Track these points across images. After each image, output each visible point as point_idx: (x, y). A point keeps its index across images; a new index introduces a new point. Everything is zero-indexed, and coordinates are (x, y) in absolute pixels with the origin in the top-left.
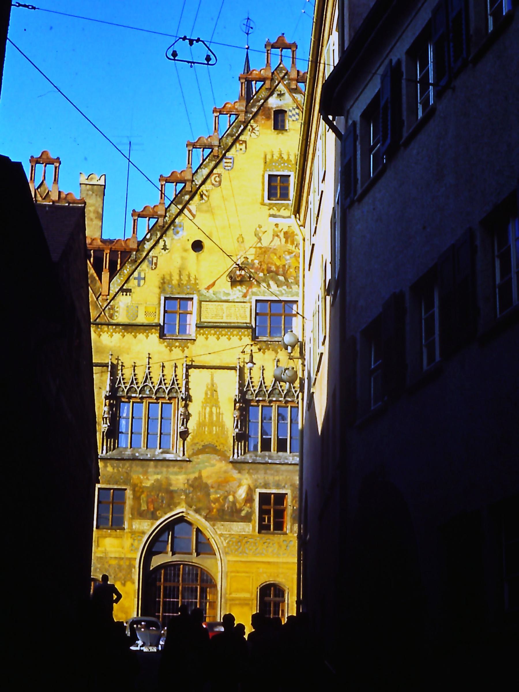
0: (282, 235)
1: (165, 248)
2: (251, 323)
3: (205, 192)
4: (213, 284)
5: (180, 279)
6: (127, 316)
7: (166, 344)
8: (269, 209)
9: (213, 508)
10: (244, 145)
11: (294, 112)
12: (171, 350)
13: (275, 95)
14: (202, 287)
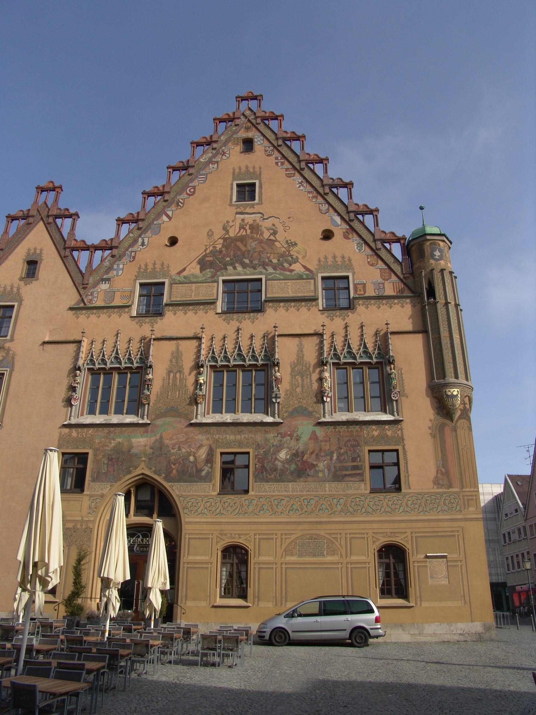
0: (247, 227)
1: (143, 244)
2: (217, 299)
3: (180, 200)
4: (184, 270)
5: (154, 268)
6: (105, 300)
7: (136, 320)
9: (173, 469)
10: (216, 165)
11: (259, 139)
14: (173, 272)
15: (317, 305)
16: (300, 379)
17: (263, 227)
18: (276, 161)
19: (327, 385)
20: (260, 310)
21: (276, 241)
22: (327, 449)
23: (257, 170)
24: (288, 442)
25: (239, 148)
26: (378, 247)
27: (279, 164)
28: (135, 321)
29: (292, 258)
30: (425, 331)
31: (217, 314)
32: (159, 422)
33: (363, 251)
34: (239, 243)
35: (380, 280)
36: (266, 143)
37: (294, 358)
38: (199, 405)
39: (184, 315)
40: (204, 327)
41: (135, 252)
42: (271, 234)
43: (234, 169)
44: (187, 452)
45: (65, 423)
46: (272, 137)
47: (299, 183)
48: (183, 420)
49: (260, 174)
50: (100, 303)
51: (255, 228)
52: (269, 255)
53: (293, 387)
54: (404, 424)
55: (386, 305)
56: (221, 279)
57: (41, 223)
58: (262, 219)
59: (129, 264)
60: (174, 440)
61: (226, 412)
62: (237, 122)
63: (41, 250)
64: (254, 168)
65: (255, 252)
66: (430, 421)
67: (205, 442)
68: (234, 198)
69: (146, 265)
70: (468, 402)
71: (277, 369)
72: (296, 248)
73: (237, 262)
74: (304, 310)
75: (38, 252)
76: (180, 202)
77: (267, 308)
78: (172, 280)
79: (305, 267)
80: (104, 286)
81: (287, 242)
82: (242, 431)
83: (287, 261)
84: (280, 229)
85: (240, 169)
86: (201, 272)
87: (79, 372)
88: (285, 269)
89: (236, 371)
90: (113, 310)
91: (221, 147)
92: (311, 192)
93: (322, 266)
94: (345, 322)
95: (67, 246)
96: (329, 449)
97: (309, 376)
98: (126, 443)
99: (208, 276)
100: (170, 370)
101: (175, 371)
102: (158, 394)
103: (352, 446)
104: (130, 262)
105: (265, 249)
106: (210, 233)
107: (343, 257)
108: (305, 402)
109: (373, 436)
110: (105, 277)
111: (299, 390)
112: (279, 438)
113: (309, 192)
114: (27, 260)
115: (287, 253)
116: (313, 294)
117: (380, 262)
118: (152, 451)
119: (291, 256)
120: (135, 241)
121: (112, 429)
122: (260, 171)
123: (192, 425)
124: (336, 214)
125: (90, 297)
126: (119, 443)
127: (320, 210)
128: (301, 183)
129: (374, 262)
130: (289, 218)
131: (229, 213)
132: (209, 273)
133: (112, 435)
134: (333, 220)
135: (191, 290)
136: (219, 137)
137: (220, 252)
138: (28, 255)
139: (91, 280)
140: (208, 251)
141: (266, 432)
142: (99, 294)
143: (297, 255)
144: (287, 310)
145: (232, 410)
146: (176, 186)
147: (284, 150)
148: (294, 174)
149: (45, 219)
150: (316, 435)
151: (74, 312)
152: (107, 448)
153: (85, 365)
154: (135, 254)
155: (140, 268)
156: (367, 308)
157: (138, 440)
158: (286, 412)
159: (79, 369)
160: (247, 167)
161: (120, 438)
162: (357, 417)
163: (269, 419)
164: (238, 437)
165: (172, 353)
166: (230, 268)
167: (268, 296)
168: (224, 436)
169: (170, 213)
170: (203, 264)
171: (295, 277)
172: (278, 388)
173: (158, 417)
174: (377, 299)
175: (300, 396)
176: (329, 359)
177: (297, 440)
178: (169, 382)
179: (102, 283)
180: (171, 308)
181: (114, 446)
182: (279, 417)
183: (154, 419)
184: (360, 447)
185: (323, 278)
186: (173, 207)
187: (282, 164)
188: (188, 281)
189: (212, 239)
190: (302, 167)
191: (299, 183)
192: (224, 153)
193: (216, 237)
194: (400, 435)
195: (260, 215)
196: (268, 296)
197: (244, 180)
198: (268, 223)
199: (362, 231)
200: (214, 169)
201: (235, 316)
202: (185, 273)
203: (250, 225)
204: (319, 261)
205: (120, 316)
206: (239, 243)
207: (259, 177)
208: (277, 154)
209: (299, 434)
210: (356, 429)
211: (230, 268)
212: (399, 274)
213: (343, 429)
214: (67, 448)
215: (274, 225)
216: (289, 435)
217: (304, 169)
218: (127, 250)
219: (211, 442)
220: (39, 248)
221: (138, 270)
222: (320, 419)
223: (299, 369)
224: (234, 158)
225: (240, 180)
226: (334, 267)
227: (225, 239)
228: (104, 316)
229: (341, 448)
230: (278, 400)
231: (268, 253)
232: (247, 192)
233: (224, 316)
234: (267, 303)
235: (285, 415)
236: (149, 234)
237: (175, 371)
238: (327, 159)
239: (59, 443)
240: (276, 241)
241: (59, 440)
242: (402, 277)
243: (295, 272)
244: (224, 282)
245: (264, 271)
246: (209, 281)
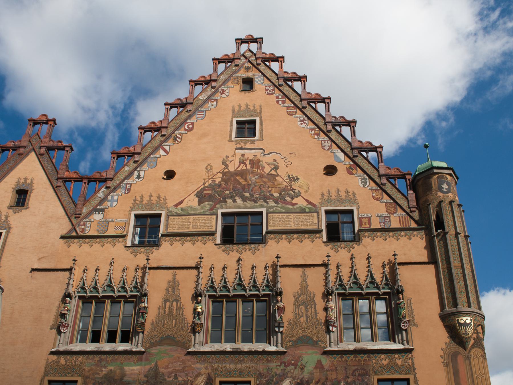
0: (248, 162)
1: (139, 177)
3: (178, 135)
4: (182, 202)
5: (151, 200)
7: (131, 250)
8: (236, 144)
10: (215, 102)
11: (260, 79)
12: (136, 255)
13: (243, 70)
14: (170, 204)
15: (321, 237)
16: (304, 309)
17: (264, 162)
18: (278, 100)
19: (333, 314)
20: (262, 241)
21: (278, 175)
22: (333, 378)
23: (258, 107)
24: (292, 371)
25: (238, 87)
26: (383, 182)
27: (280, 102)
28: (129, 251)
29: (294, 192)
31: (216, 244)
32: (154, 350)
33: (367, 186)
34: (238, 178)
35: (386, 214)
36: (267, 83)
37: (297, 288)
38: (197, 334)
39: (181, 245)
40: (202, 256)
41: (131, 184)
42: (272, 169)
43: (233, 107)
44: (184, 381)
45: (53, 350)
46: (273, 78)
47: (301, 121)
48: (179, 349)
49: (261, 112)
50: (91, 233)
51: (255, 163)
52: (270, 189)
53: (296, 317)
54: (414, 353)
55: (393, 237)
56: (220, 211)
57: (33, 154)
58: (262, 154)
59: (123, 195)
60: (170, 368)
61: (225, 342)
62: (237, 62)
63: (32, 180)
64: (254, 106)
65: (255, 186)
66: (442, 349)
67: (203, 371)
68: (234, 134)
69: (142, 197)
70: (481, 332)
71: (279, 298)
72: (298, 183)
73: (237, 195)
74: (307, 242)
75: (29, 181)
76: (177, 137)
77: (269, 240)
78: (169, 212)
79: (307, 201)
80: (98, 217)
81: (289, 176)
82: (243, 360)
83: (289, 195)
84: (281, 164)
85: (240, 106)
86: (199, 205)
87: (68, 299)
88: (287, 203)
89: (236, 301)
90: (106, 239)
91: (220, 86)
92: (313, 129)
93: (326, 199)
94: (351, 253)
95: (59, 176)
96: (335, 378)
97: (313, 306)
98: (118, 371)
99: (207, 209)
100: (167, 298)
101: (171, 300)
102: (153, 322)
103: (359, 375)
104: (125, 193)
105: (265, 183)
106: (209, 168)
107: (347, 192)
108: (309, 331)
109: (382, 365)
110: (98, 208)
111: (303, 319)
112: (282, 367)
113: (311, 130)
114: (16, 189)
115: (289, 187)
116: (316, 227)
117: (385, 196)
118: (146, 379)
119: (294, 191)
120: (131, 174)
121: (103, 357)
122: (261, 108)
123: (189, 353)
124: (339, 151)
125: (83, 227)
126: (111, 370)
127: (322, 146)
128: (303, 121)
129: (379, 197)
130: (291, 154)
131: (229, 149)
132: (208, 206)
133: (103, 363)
134: (335, 156)
135: (189, 222)
136: (218, 76)
137: (220, 185)
138: (18, 185)
139: (85, 211)
140: (206, 185)
141: (268, 361)
142: (93, 224)
143: (299, 189)
144: (290, 242)
145: (231, 339)
146: (173, 122)
147: (285, 89)
148: (296, 112)
149: (37, 150)
151: (65, 240)
152: (98, 376)
153: (76, 293)
154: (131, 186)
155: (135, 200)
156: (373, 240)
157: (131, 368)
158: (290, 341)
159: (69, 296)
160: (247, 105)
161: (112, 366)
162: (365, 347)
163: (273, 348)
164: (239, 366)
165: (169, 283)
166: (230, 201)
167: (269, 228)
168: (224, 365)
169: (167, 148)
170: (201, 197)
171: (298, 210)
172: (281, 317)
173: (153, 345)
174: (383, 231)
175: (304, 325)
176: (334, 289)
177: (302, 369)
178: (165, 311)
179: (96, 214)
180: (167, 238)
181: (105, 374)
182: (282, 346)
183: (149, 347)
184: (369, 375)
185: (327, 212)
186: (171, 142)
187: (284, 102)
188: (185, 213)
189: (211, 173)
190: (304, 105)
191: (301, 121)
192: (223, 92)
193: (215, 171)
194: (410, 364)
195: (261, 151)
196: (269, 228)
197: (244, 117)
198: (269, 159)
199: (366, 167)
200: (213, 107)
201: (235, 247)
202: (182, 206)
203: (250, 160)
204: (323, 195)
205: (114, 246)
206: (238, 178)
207: (259, 114)
208: (277, 93)
210: (364, 358)
211: (230, 201)
212: (405, 208)
213: (350, 359)
214: (55, 375)
215: (275, 160)
216: (293, 365)
217: (306, 107)
218: (122, 182)
219: (210, 371)
220: (30, 177)
221: (133, 202)
222: (325, 348)
223: (304, 299)
224: (234, 97)
225: (240, 117)
226: (338, 201)
227: (224, 174)
228: (96, 245)
229: (348, 378)
230: (281, 330)
231: (269, 187)
232: (246, 128)
233: (223, 247)
234: (269, 235)
235: (289, 344)
236: (145, 167)
237: (171, 300)
238: (329, 98)
239: (45, 370)
240: (278, 175)
241: (45, 368)
242: (408, 211)
243: (297, 206)
244: (224, 215)
245: (265, 204)
246: (207, 213)
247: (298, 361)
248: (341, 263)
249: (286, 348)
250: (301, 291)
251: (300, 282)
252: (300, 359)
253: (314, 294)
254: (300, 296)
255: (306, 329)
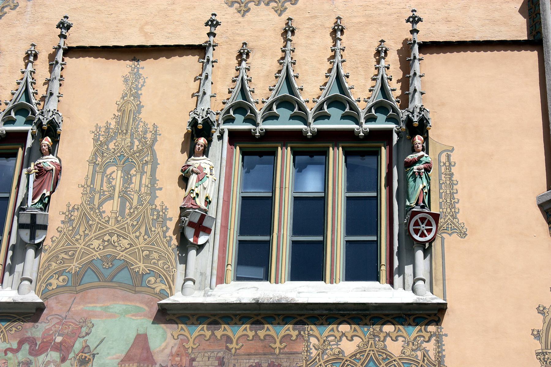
16: (118, 175)
30: (535, 41)
37: (108, 115)
53: (93, 199)
54: (447, 320)
94: (285, 16)
109: (338, 357)
111: (110, 207)
150: (148, 349)
158: (60, 273)
175: (112, 226)
177: (84, 361)
194: (432, 354)
209: (92, 341)
216: (58, 348)
247: (76, 334)
248: (250, 45)
249: (44, 294)
250: (120, 121)
251: (117, 98)
252: (84, 330)
253: (155, 133)
254: (112, 138)
255: (115, 238)
